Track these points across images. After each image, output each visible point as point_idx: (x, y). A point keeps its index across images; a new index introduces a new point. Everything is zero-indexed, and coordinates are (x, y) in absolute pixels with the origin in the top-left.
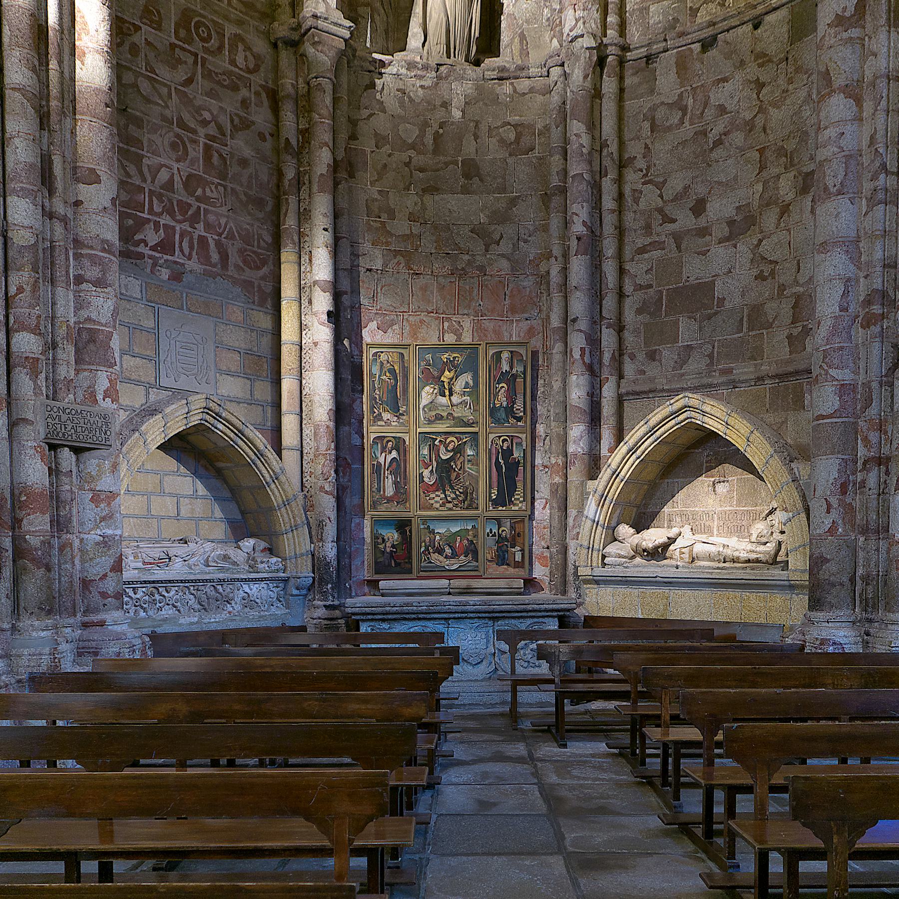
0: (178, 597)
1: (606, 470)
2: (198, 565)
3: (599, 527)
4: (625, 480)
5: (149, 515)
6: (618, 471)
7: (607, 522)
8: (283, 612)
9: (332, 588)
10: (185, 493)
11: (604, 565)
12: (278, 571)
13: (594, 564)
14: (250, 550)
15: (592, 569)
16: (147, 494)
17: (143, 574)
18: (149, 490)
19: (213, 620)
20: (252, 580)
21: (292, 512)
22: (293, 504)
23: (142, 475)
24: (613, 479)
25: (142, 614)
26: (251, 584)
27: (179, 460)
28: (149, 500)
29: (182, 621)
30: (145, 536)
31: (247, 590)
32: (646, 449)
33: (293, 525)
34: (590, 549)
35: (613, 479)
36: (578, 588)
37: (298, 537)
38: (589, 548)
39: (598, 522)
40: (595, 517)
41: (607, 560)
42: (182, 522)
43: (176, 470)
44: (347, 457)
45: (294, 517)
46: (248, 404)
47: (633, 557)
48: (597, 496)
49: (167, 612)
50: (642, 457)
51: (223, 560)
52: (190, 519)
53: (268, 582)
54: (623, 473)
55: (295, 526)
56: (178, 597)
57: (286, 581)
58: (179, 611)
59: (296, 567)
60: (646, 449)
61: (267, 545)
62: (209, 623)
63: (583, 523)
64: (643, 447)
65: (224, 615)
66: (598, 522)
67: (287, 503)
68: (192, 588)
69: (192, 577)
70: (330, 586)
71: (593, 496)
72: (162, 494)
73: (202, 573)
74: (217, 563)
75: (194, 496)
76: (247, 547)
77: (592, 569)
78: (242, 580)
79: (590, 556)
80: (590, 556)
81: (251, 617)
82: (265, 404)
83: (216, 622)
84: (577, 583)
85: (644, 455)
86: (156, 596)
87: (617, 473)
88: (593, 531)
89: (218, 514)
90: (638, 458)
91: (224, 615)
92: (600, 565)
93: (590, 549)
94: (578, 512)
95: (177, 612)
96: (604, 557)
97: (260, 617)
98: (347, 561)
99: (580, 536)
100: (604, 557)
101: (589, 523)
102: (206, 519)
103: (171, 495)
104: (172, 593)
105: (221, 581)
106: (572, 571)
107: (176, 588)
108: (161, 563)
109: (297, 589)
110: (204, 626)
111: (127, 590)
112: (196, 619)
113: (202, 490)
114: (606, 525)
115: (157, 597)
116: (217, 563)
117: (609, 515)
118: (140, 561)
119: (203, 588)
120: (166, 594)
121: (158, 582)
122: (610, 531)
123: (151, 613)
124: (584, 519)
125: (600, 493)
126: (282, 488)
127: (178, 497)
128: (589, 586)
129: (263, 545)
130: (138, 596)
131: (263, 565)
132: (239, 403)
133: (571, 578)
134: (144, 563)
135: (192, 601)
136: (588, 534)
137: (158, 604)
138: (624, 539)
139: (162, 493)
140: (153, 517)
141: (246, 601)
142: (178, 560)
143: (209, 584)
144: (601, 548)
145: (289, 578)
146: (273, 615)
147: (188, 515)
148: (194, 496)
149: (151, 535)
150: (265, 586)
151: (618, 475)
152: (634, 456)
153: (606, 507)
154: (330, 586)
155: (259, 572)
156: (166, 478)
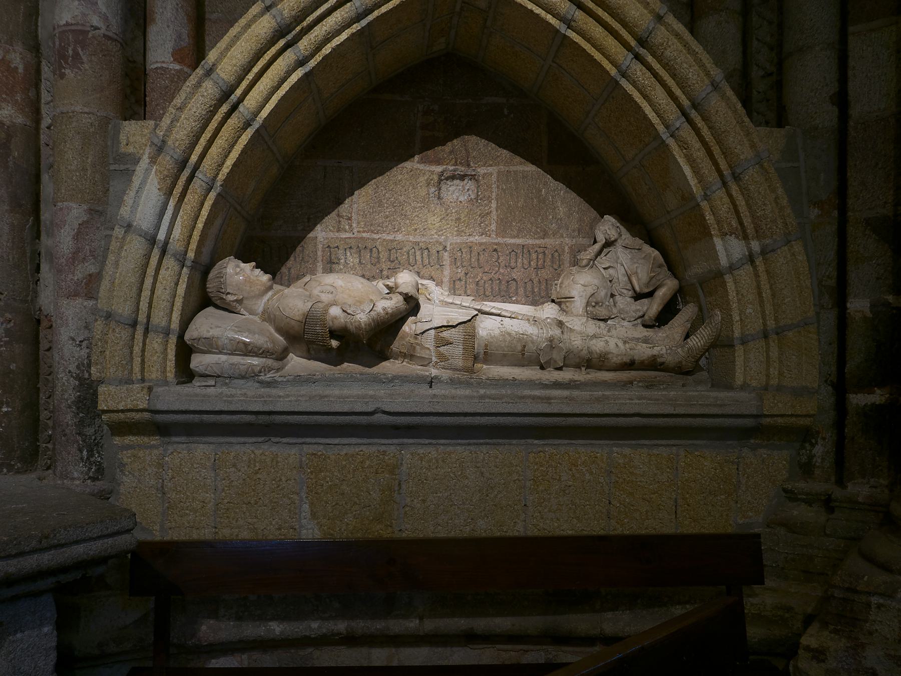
1: (198, 85)
3: (170, 263)
4: (256, 125)
6: (239, 92)
7: (193, 246)
11: (186, 374)
13: (154, 374)
15: (150, 389)
24: (218, 117)
32: (327, 40)
34: (140, 330)
35: (218, 117)
36: (93, 446)
38: (134, 324)
39: (166, 243)
40: (158, 227)
41: (198, 362)
47: (281, 356)
48: (167, 161)
50: (312, 63)
54: (251, 102)
60: (327, 40)
63: (114, 245)
64: (319, 32)
66: (166, 243)
71: (153, 160)
77: (150, 389)
79: (137, 349)
80: (137, 349)
84: (89, 431)
85: (318, 58)
87: (234, 98)
88: (151, 271)
90: (301, 63)
92: (171, 375)
93: (140, 330)
94: (91, 211)
96: (185, 351)
99: (105, 284)
100: (185, 351)
101: (135, 247)
106: (71, 395)
114: (191, 255)
117: (200, 225)
122: (198, 276)
124: (118, 232)
125: (178, 153)
128: (130, 439)
133: (68, 418)
136: (133, 279)
138: (239, 301)
144: (175, 324)
151: (234, 108)
152: (289, 57)
153: (191, 198)
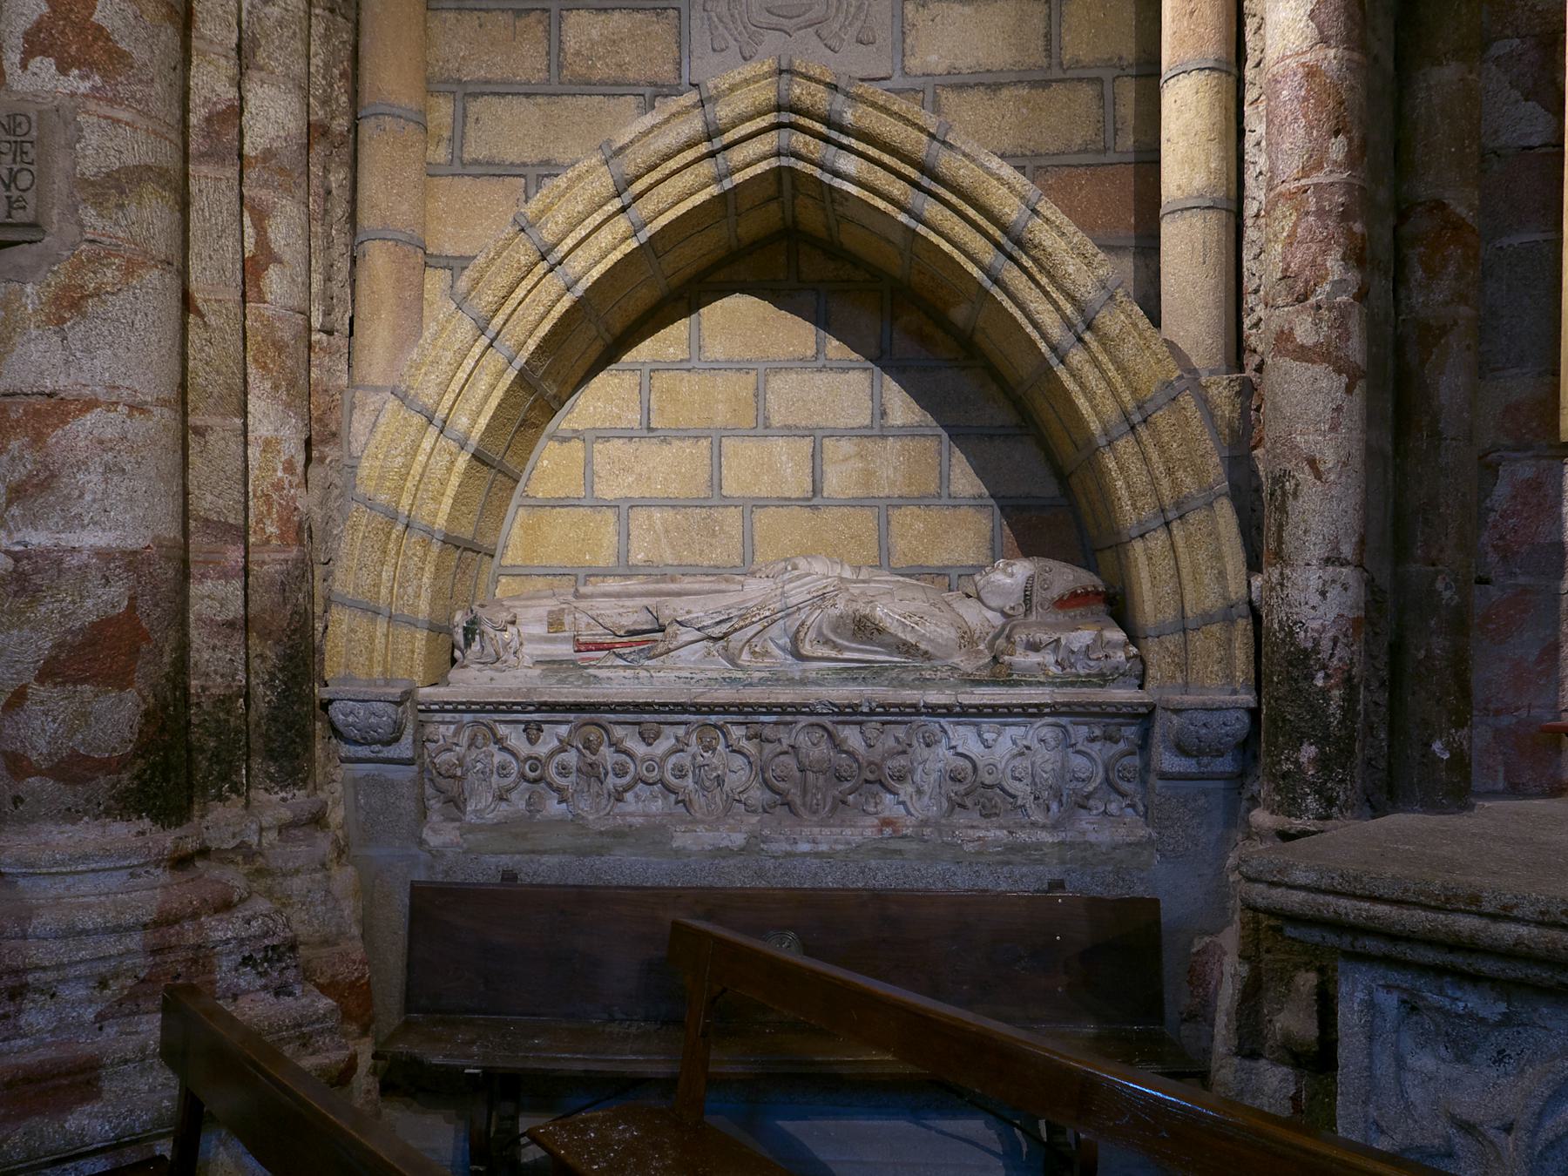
0: (684, 759)
2: (766, 654)
5: (714, 497)
8: (1120, 835)
9: (1322, 762)
10: (841, 423)
12: (1103, 679)
14: (1013, 601)
16: (715, 437)
17: (561, 681)
18: (719, 421)
19: (804, 847)
20: (994, 711)
21: (1162, 449)
22: (1162, 419)
23: (694, 377)
25: (554, 807)
26: (989, 728)
27: (823, 321)
28: (717, 455)
29: (682, 840)
30: (699, 560)
31: (973, 747)
33: (1167, 501)
37: (1190, 547)
42: (828, 515)
43: (810, 353)
44: (1449, 197)
45: (1170, 472)
46: (1034, 85)
49: (642, 807)
51: (854, 636)
52: (856, 503)
53: (1063, 721)
55: (1178, 505)
56: (684, 759)
57: (1144, 717)
58: (686, 804)
59: (1184, 666)
61: (1088, 580)
62: (788, 855)
65: (862, 831)
67: (1135, 421)
68: (737, 732)
69: (724, 695)
70: (1308, 752)
72: (760, 431)
73: (775, 680)
74: (835, 646)
75: (878, 429)
76: (1001, 591)
78: (933, 710)
81: (968, 847)
82: (1107, 75)
83: (818, 855)
86: (605, 750)
89: (965, 480)
91: (862, 831)
95: (681, 809)
97: (1012, 849)
98: (1439, 645)
102: (922, 501)
103: (791, 432)
104: (663, 746)
105: (848, 713)
107: (681, 731)
108: (629, 645)
109: (1181, 749)
110: (770, 864)
111: (502, 730)
112: (739, 839)
113: (901, 407)
115: (607, 755)
116: (840, 649)
118: (565, 640)
119: (782, 733)
120: (640, 749)
121: (611, 708)
123: (584, 806)
126: (1114, 360)
127: (817, 437)
129: (1066, 577)
130: (542, 750)
131: (1034, 658)
132: (995, 87)
134: (581, 647)
135: (738, 774)
137: (611, 781)
139: (763, 428)
140: (727, 502)
141: (961, 788)
142: (687, 635)
143: (804, 720)
145: (1152, 709)
146: (1072, 845)
147: (851, 493)
148: (878, 429)
149: (717, 556)
150: (1047, 733)
154: (1308, 752)
155: (1017, 684)
156: (776, 383)
